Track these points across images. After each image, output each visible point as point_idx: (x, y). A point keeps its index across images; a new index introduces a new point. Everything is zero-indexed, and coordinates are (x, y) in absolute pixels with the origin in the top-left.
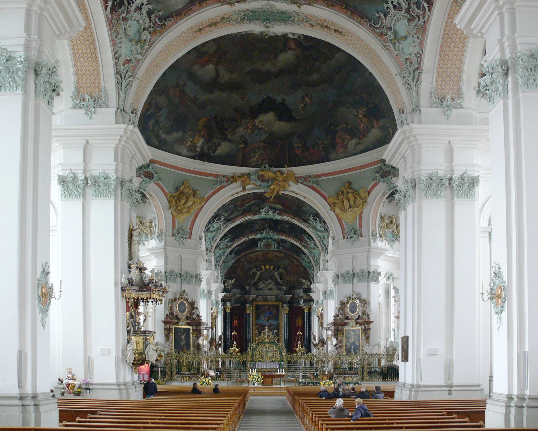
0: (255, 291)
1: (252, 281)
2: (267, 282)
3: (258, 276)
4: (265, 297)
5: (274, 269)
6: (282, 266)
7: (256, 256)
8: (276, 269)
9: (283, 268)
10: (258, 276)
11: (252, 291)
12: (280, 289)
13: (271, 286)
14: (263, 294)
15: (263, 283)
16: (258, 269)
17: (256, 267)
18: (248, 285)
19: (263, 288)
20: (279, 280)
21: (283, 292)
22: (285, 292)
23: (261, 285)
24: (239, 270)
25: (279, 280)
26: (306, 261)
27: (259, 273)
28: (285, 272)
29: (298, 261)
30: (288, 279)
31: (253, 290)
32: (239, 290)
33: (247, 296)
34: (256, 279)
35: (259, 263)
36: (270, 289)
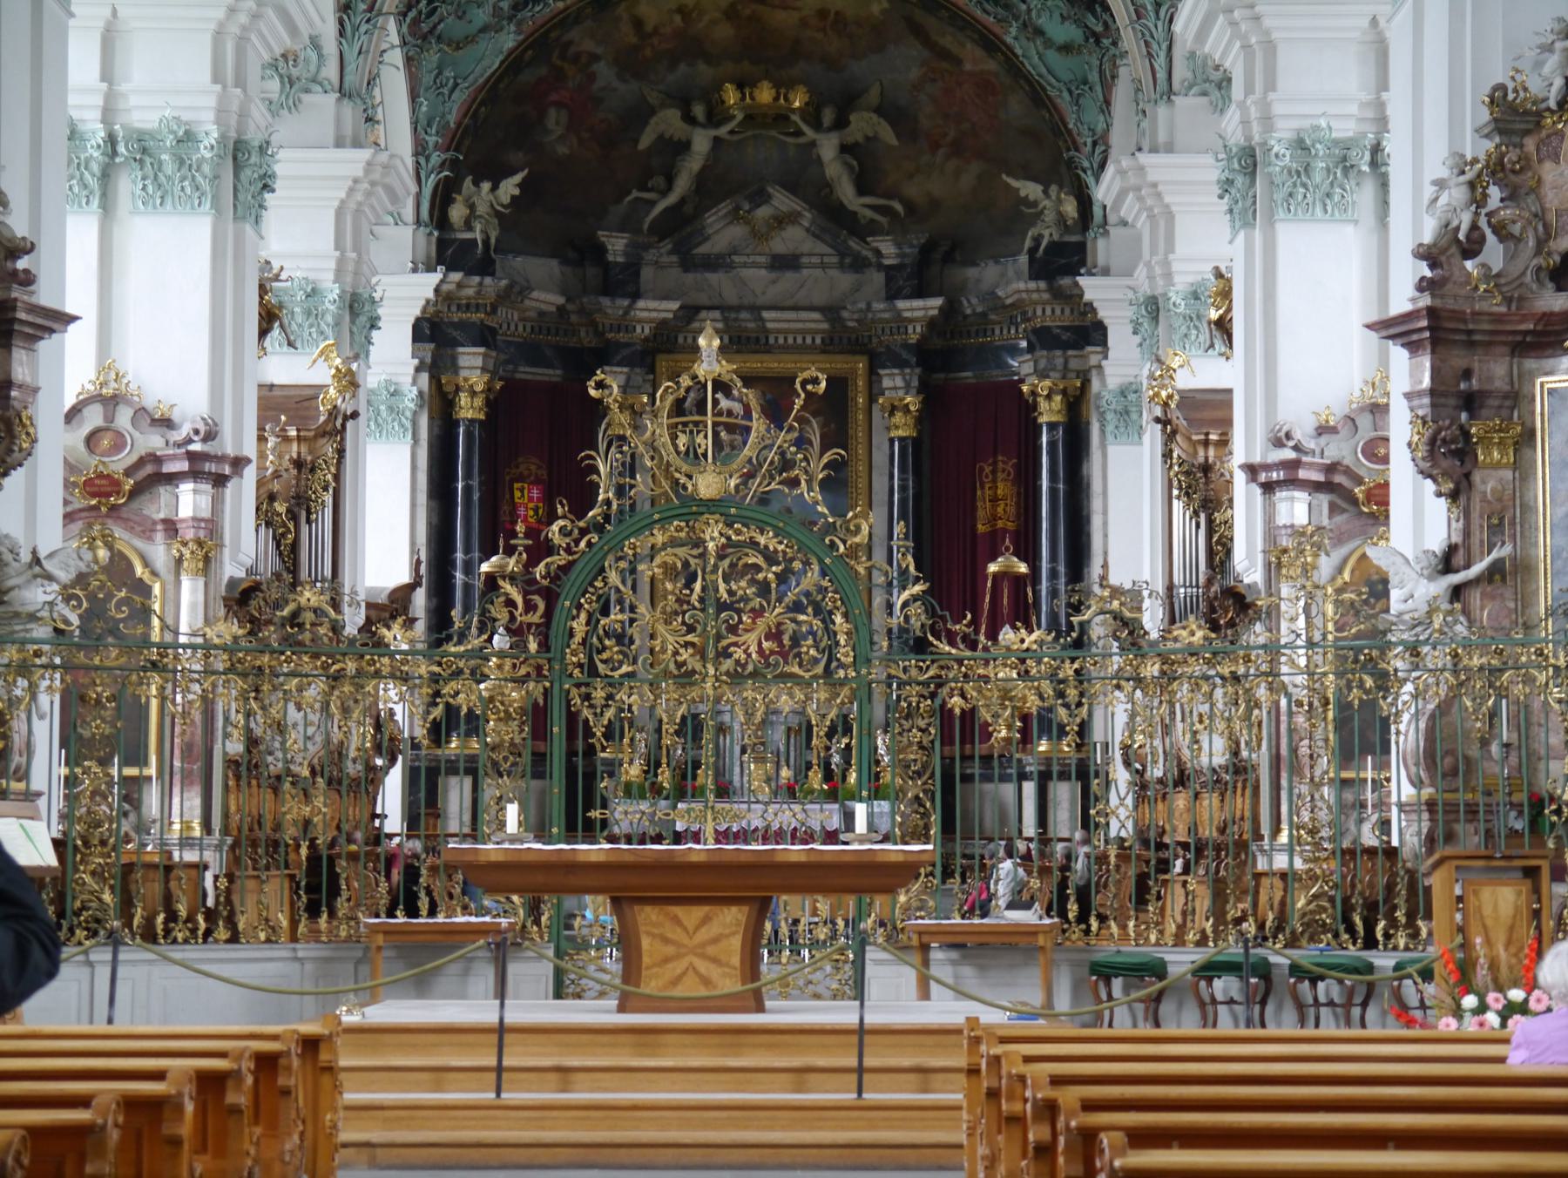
0: (675, 272)
1: (653, 203)
2: (763, 212)
3: (693, 164)
4: (746, 319)
5: (812, 115)
6: (873, 96)
7: (681, 10)
8: (828, 116)
9: (879, 111)
10: (693, 164)
11: (647, 273)
12: (858, 265)
13: (793, 239)
14: (730, 295)
15: (735, 216)
16: (699, 111)
17: (684, 104)
18: (622, 229)
19: (735, 251)
20: (846, 192)
21: (878, 278)
22: (889, 280)
23: (721, 232)
24: (555, 120)
25: (846, 192)
26: (1049, 43)
27: (701, 142)
28: (887, 135)
29: (991, 44)
30: (912, 190)
31: (659, 265)
32: (554, 263)
33: (612, 307)
34: (682, 184)
35: (704, 71)
36: (785, 263)
